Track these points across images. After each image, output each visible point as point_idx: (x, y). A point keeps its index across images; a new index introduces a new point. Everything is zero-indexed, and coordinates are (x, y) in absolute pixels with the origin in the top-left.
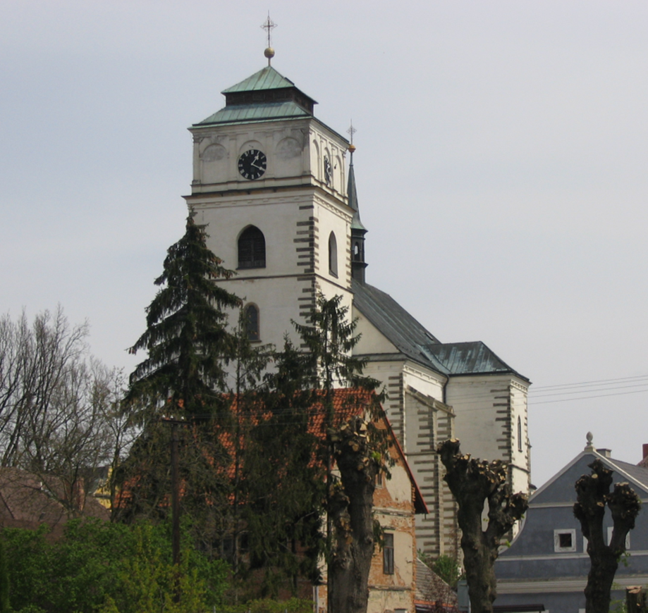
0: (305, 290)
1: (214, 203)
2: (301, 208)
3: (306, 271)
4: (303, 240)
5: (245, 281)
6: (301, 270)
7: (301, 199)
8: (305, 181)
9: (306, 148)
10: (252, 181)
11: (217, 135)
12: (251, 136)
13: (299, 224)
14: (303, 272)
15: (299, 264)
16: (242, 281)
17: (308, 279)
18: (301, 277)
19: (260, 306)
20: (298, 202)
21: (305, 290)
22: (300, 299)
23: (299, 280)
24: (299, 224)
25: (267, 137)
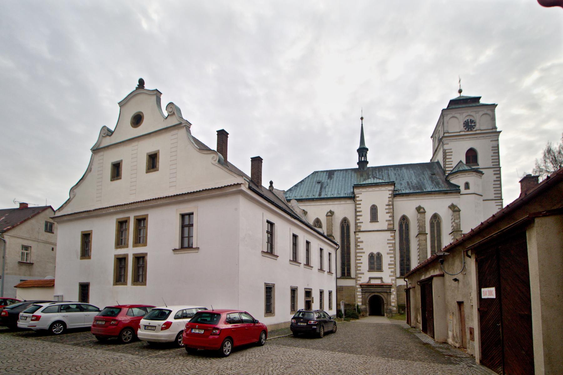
8: (494, 130)
10: (468, 131)
12: (469, 113)
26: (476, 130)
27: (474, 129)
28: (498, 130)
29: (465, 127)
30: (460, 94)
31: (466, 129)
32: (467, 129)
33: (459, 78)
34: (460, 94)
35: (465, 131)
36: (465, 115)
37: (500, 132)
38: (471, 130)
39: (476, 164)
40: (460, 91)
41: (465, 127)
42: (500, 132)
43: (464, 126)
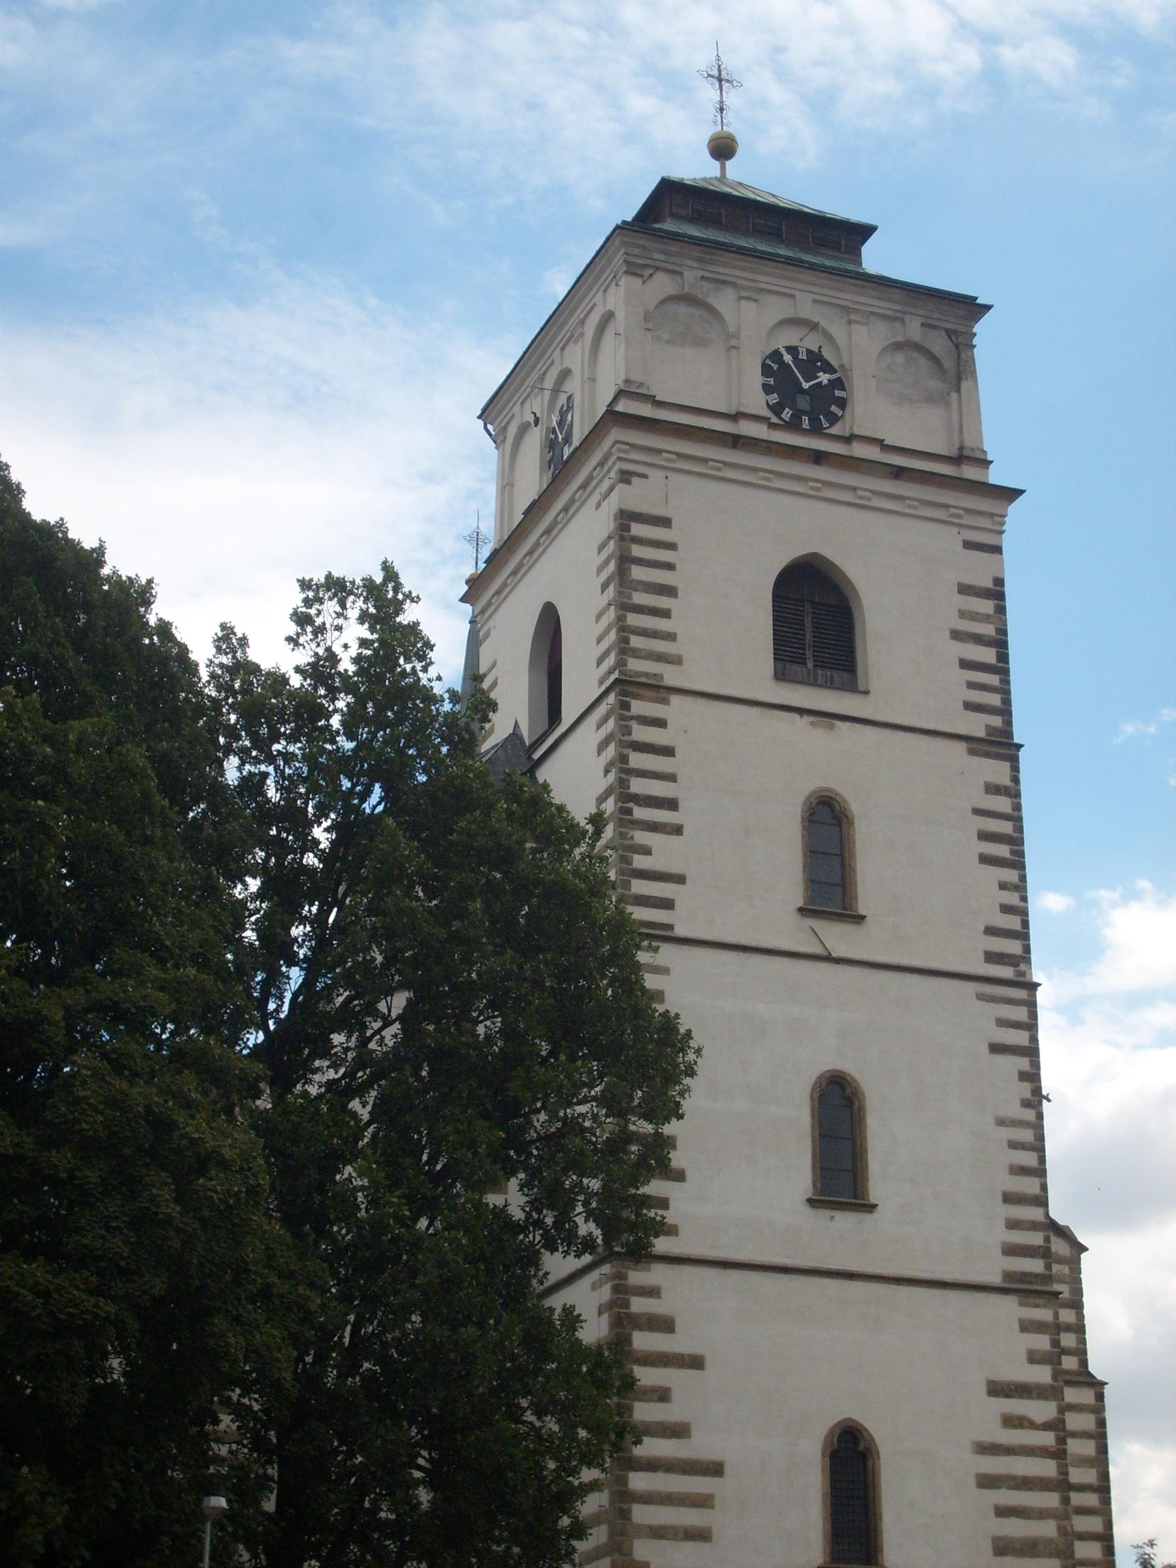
0: (993, 789)
1: (705, 461)
2: (968, 545)
3: (990, 729)
4: (978, 639)
5: (807, 719)
6: (976, 726)
7: (967, 520)
8: (969, 472)
9: (965, 385)
10: (793, 426)
11: (700, 273)
12: (805, 308)
13: (965, 590)
14: (981, 733)
15: (969, 706)
16: (796, 716)
17: (997, 757)
18: (976, 745)
19: (855, 808)
20: (960, 526)
21: (993, 789)
22: (977, 812)
23: (972, 752)
24: (965, 590)
25: (850, 322)
26: (849, 439)
27: (835, 430)
28: (996, 476)
29: (774, 398)
30: (723, 168)
31: (776, 409)
32: (787, 414)
33: (718, 58)
34: (723, 168)
35: (774, 420)
36: (777, 309)
37: (1013, 494)
38: (816, 430)
39: (846, 676)
40: (723, 149)
41: (774, 398)
42: (1013, 494)
43: (767, 389)
